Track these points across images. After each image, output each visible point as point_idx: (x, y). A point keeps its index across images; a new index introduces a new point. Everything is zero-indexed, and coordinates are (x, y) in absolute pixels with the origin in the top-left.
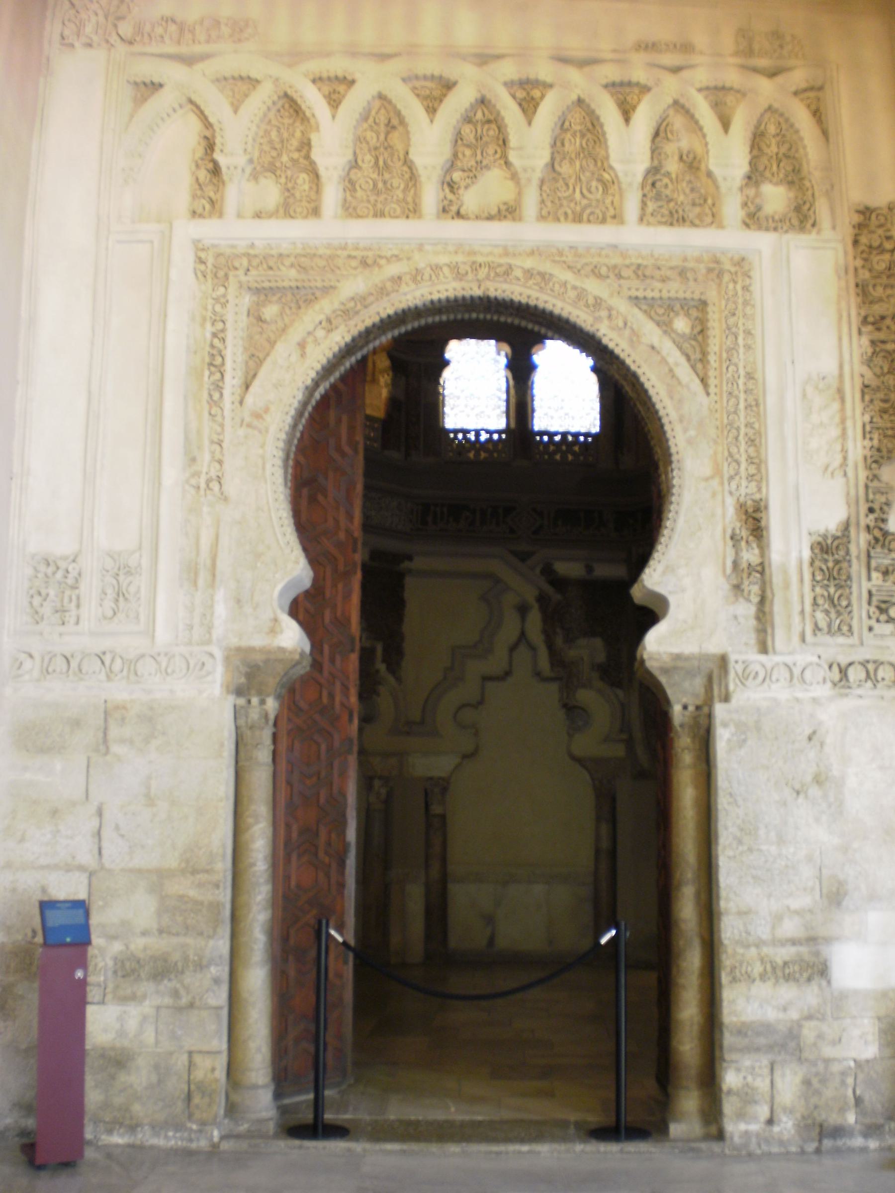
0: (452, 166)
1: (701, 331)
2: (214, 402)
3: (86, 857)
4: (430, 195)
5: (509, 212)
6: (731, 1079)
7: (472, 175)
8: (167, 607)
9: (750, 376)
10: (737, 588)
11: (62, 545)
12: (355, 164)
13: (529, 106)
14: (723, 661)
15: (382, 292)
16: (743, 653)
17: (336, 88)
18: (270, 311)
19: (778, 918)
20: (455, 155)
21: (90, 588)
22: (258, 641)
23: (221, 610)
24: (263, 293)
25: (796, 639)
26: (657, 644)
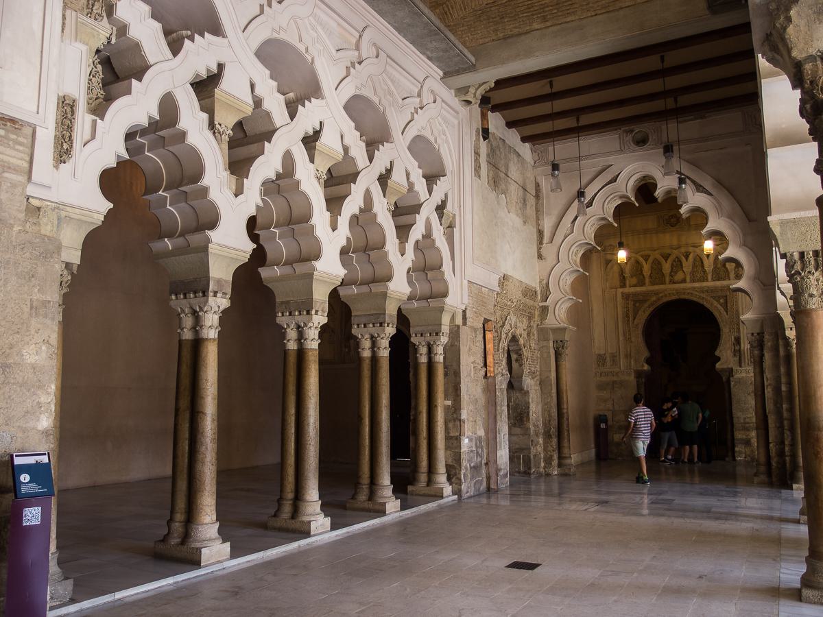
0: (671, 272)
1: (726, 302)
2: (628, 324)
3: (611, 408)
4: (667, 279)
5: (684, 281)
6: (737, 449)
7: (676, 273)
8: (622, 363)
9: (737, 311)
10: (735, 355)
11: (602, 352)
12: (651, 273)
13: (687, 257)
14: (732, 369)
15: (659, 299)
16: (736, 368)
17: (646, 258)
18: (637, 305)
19: (745, 419)
20: (672, 270)
21: (608, 360)
22: (640, 369)
23: (632, 362)
24: (635, 302)
25: (746, 365)
26: (718, 366)
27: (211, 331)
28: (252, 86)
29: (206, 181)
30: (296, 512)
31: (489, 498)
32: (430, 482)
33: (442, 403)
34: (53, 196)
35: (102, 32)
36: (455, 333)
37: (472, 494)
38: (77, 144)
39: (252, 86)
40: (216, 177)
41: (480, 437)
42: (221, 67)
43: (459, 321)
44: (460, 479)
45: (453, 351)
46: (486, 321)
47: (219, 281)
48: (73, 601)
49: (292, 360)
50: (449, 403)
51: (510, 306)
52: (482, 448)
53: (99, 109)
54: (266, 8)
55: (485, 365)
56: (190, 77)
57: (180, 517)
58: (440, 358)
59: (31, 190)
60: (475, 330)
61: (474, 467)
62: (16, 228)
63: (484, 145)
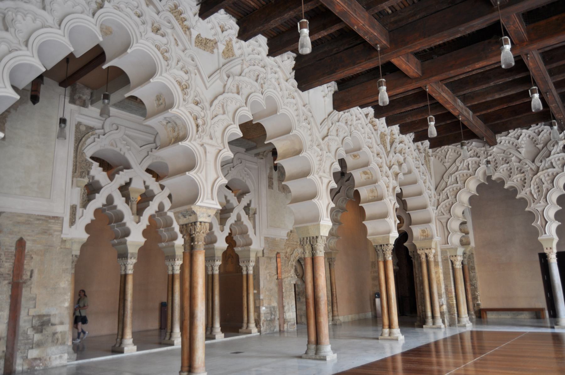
11: (374, 260)
27: (130, 272)
28: (144, 182)
29: (124, 221)
30: (171, 336)
31: (280, 334)
32: (248, 327)
33: (252, 291)
34: (69, 237)
35: (86, 181)
36: (257, 260)
37: (268, 332)
38: (77, 219)
39: (144, 182)
40: (129, 219)
41: (274, 307)
42: (131, 179)
43: (260, 254)
44: (260, 326)
45: (256, 269)
46: (278, 253)
47: (132, 254)
48: (77, 360)
49: (170, 278)
50: (256, 292)
51: (297, 245)
52: (275, 312)
53: (84, 206)
54: (150, 153)
55: (277, 274)
56: (118, 186)
57: (120, 337)
58: (251, 272)
59: (62, 236)
60: (270, 258)
61: (270, 320)
62: (58, 248)
63: (275, 174)
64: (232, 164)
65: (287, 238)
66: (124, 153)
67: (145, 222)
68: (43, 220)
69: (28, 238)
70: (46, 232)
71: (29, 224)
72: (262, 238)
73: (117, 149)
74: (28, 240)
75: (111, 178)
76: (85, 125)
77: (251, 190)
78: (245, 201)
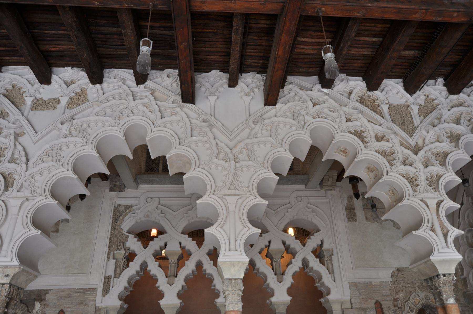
28: (180, 244)
39: (180, 244)
43: (348, 305)
64: (289, 205)
65: (391, 280)
66: (159, 221)
67: (180, 282)
68: (81, 292)
69: (68, 309)
70: (82, 303)
71: (69, 297)
72: (346, 284)
73: (153, 219)
74: (67, 311)
75: (145, 246)
76: (124, 206)
77: (321, 228)
78: (313, 242)
